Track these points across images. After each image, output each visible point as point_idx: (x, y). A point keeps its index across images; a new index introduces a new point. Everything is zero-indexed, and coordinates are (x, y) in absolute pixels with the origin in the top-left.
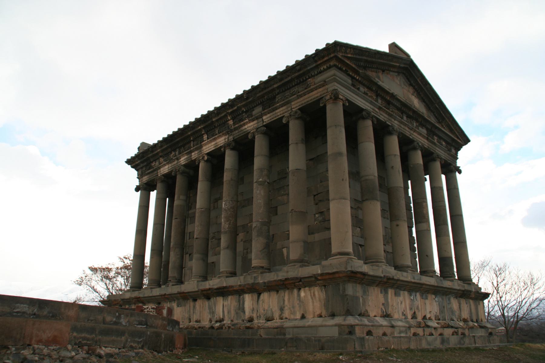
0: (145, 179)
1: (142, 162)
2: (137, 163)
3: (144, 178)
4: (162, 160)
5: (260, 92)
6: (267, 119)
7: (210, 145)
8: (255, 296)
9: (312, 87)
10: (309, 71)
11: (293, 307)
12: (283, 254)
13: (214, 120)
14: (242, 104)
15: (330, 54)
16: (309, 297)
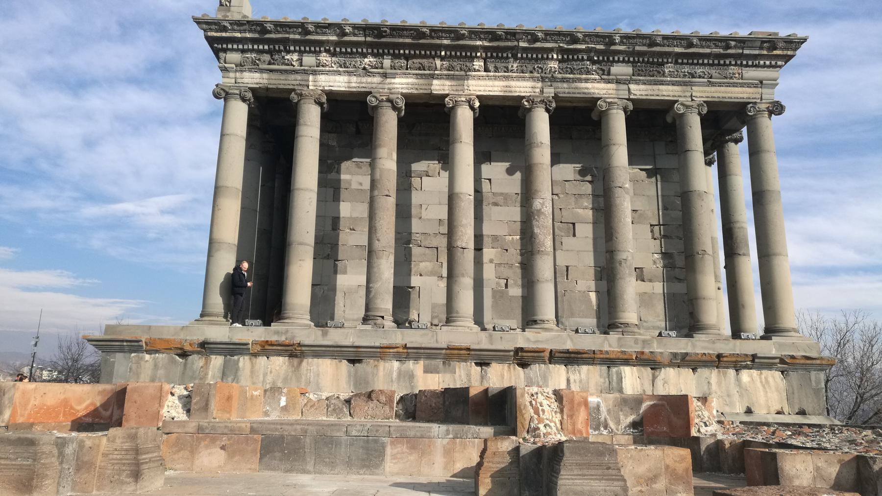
0: (253, 79)
1: (253, 41)
2: (238, 35)
3: (247, 75)
4: (325, 58)
5: (644, 45)
6: (640, 91)
7: (490, 83)
8: (647, 372)
9: (735, 80)
10: (741, 56)
11: (729, 396)
12: (590, 301)
13: (523, 44)
14: (598, 47)
15: (788, 49)
16: (759, 384)
